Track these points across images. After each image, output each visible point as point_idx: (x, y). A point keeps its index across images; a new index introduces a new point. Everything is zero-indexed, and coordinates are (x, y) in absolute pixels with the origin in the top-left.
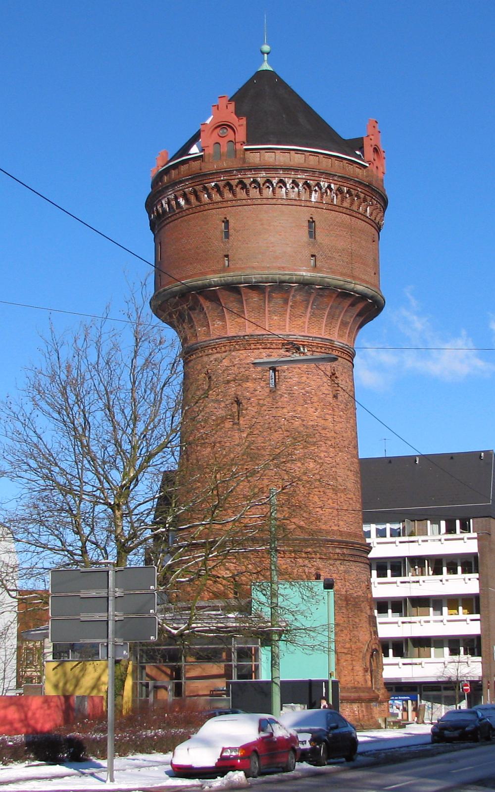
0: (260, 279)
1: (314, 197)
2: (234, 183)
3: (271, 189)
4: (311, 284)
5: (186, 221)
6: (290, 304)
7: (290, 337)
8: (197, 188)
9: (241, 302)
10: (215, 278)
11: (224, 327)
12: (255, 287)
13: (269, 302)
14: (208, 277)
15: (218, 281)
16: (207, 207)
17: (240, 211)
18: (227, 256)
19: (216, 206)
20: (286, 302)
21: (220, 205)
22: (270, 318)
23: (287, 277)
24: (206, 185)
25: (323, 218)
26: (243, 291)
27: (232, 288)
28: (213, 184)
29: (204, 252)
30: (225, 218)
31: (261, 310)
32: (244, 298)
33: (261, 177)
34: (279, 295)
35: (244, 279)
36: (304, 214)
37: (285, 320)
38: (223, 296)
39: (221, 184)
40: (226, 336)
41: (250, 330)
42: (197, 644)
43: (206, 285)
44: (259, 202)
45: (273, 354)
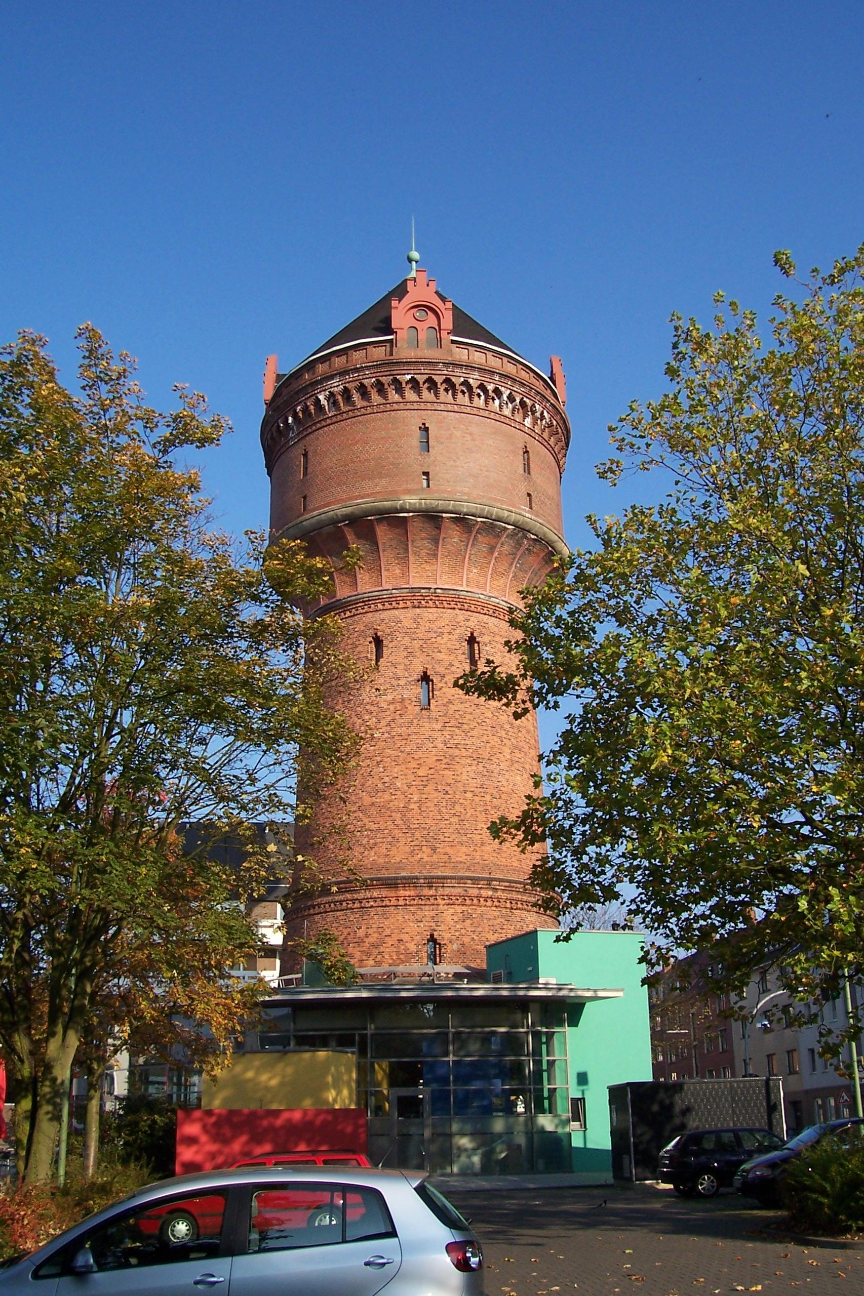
0: (474, 511)
1: (528, 422)
2: (439, 379)
3: (483, 397)
4: (529, 531)
5: (360, 422)
6: (496, 554)
7: (492, 599)
8: (383, 379)
9: (436, 541)
10: (411, 500)
11: (405, 573)
12: (462, 521)
13: (473, 545)
14: (403, 497)
15: (415, 504)
16: (395, 406)
17: (444, 418)
18: (426, 474)
19: (409, 406)
20: (492, 549)
21: (416, 406)
22: (469, 570)
23: (506, 513)
24: (398, 377)
25: (536, 448)
26: (447, 524)
27: (432, 518)
28: (408, 377)
29: (393, 464)
30: (424, 424)
31: (459, 556)
32: (442, 535)
33: (474, 379)
34: (486, 540)
35: (453, 506)
36: (521, 438)
37: (486, 576)
38: (383, 533)
39: (421, 379)
40: (407, 586)
41: (444, 581)
42: (631, 1172)
43: (396, 508)
44: (468, 410)
45: (472, 619)
